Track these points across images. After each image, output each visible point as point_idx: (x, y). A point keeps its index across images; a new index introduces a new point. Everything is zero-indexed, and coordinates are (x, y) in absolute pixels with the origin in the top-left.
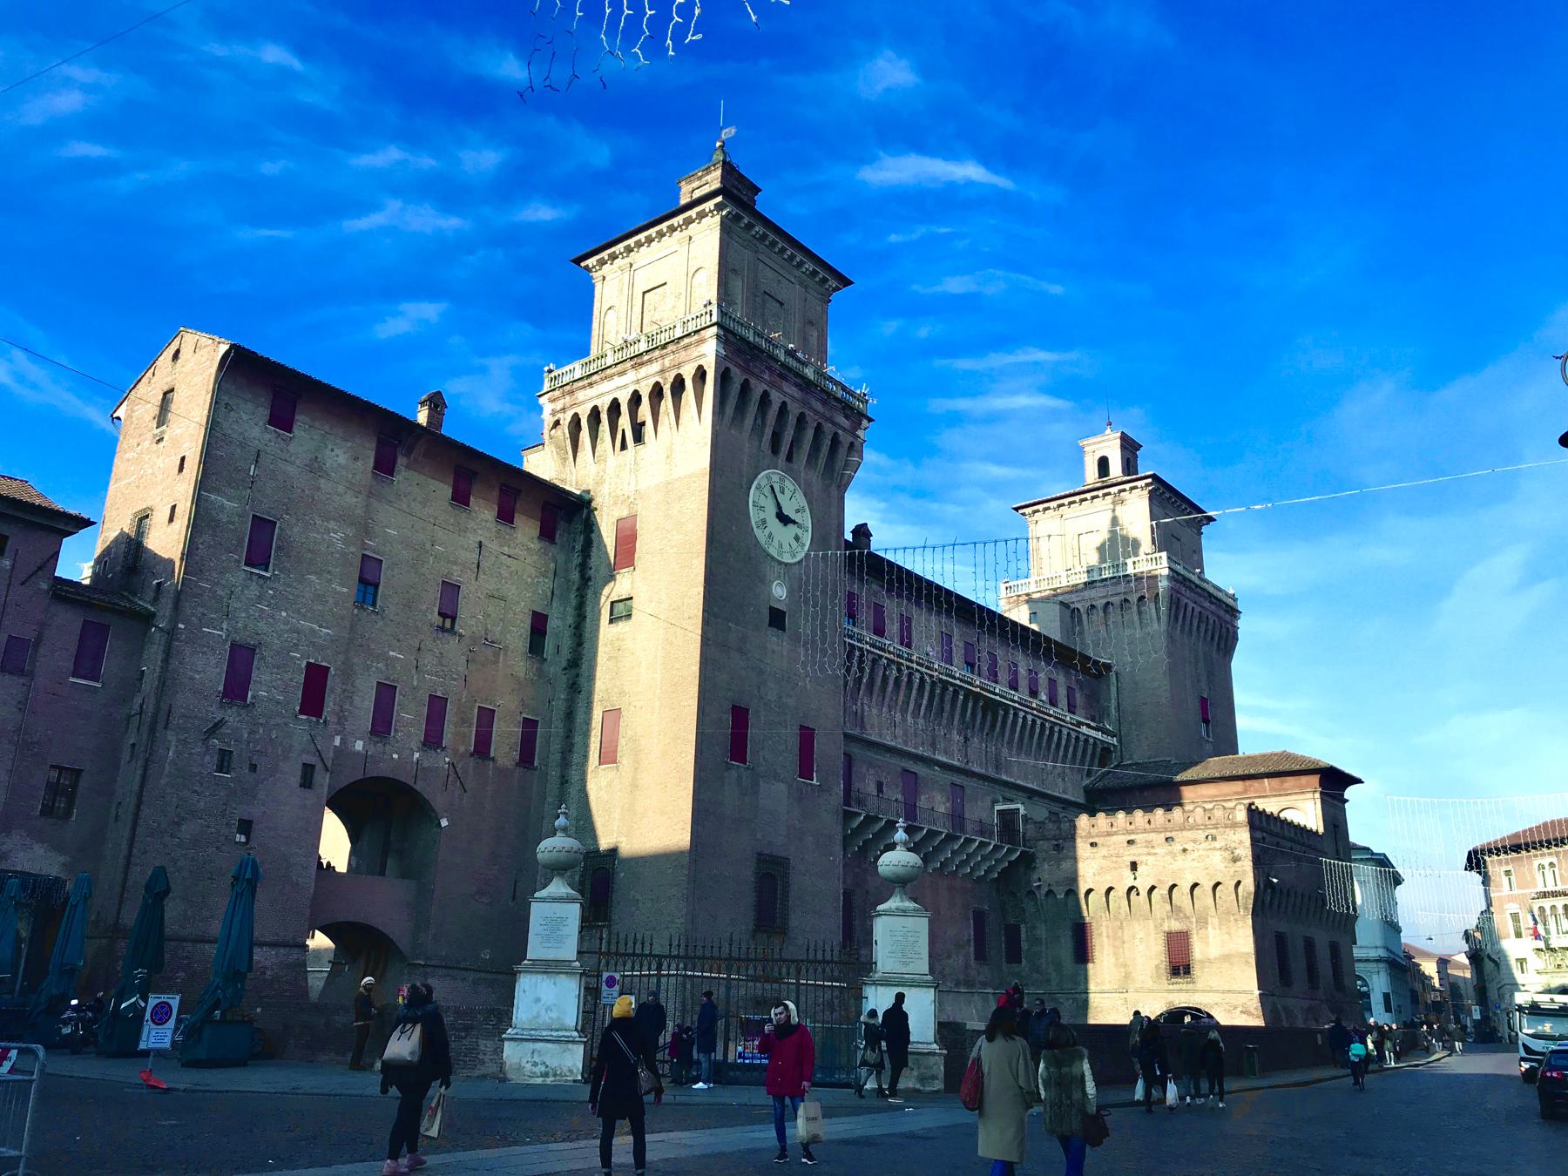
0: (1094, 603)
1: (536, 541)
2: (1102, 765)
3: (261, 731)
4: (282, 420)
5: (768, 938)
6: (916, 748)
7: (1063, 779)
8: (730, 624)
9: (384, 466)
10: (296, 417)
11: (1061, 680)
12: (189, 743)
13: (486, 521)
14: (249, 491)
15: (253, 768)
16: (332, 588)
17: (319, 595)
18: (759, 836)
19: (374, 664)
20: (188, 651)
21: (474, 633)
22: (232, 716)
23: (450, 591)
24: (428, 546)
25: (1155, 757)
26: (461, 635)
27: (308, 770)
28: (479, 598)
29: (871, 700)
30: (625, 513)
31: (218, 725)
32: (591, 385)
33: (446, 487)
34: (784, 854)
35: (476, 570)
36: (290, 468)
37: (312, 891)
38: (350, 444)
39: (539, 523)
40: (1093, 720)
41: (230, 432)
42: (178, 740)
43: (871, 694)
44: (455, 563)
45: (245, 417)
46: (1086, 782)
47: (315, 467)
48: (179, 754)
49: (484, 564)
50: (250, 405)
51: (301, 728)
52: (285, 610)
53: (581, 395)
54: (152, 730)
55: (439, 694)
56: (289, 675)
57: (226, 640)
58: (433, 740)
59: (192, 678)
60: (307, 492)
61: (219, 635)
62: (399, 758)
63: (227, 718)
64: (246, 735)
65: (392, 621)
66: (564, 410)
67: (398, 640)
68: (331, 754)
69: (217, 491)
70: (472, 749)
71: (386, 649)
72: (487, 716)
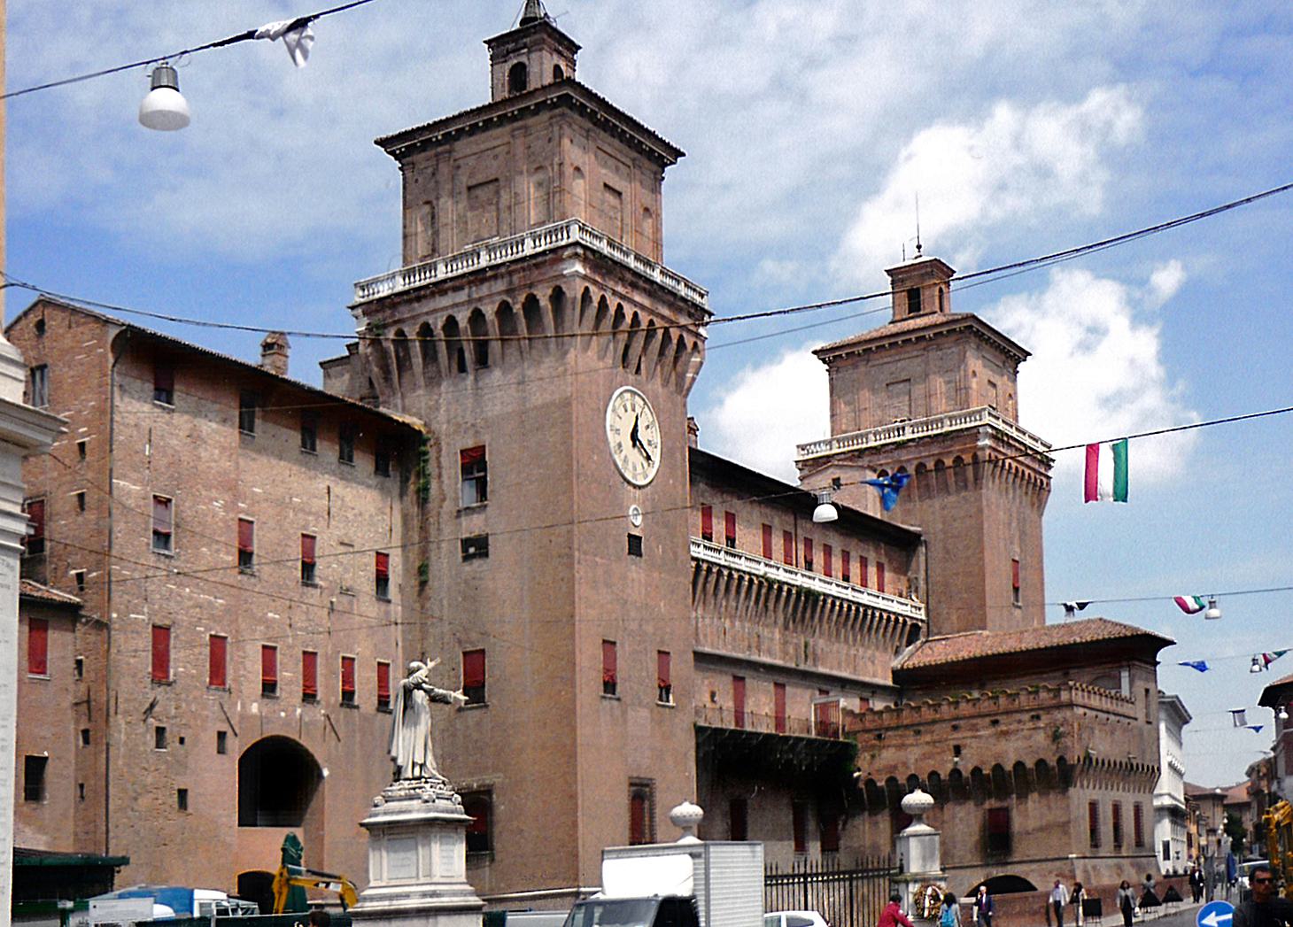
0: (904, 465)
1: (373, 476)
2: (909, 644)
3: (184, 705)
4: (163, 393)
6: (744, 653)
7: (873, 662)
9: (246, 425)
10: (176, 387)
11: (872, 556)
13: (331, 464)
14: (147, 471)
15: (182, 741)
22: (160, 693)
23: (308, 539)
24: (287, 500)
25: (965, 630)
26: (321, 587)
27: (221, 736)
30: (470, 444)
31: (152, 706)
32: (418, 299)
35: (326, 517)
36: (174, 442)
39: (374, 457)
40: (901, 596)
44: (310, 513)
46: (896, 663)
47: (194, 438)
49: (332, 510)
51: (212, 697)
52: (188, 586)
53: (404, 312)
54: (108, 715)
55: (310, 650)
57: (148, 624)
58: (309, 697)
59: (129, 664)
61: (144, 620)
63: (158, 698)
66: (385, 326)
68: (237, 719)
71: (265, 611)
72: (348, 663)
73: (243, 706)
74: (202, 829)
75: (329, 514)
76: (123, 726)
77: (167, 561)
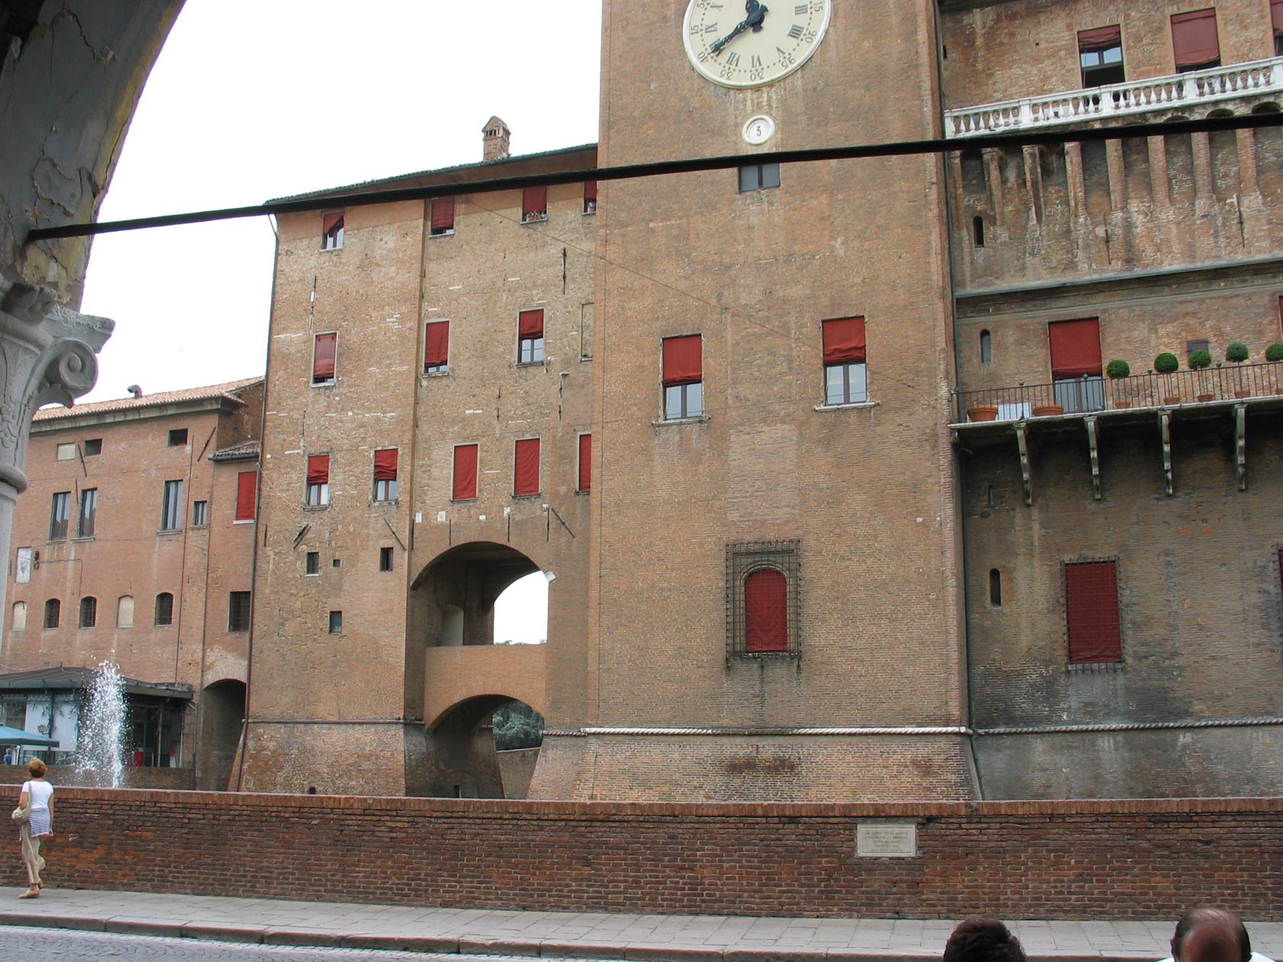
5: (762, 667)
8: (651, 225)
12: (284, 554)
14: (311, 316)
15: (336, 563)
16: (392, 371)
17: (380, 383)
18: (733, 516)
19: (451, 430)
20: (275, 475)
21: (565, 354)
22: (314, 522)
24: (500, 283)
26: (549, 363)
27: (386, 554)
28: (569, 312)
29: (1152, 200)
33: (514, 210)
34: (789, 533)
37: (404, 669)
38: (397, 224)
41: (291, 274)
42: (276, 554)
43: (1149, 188)
44: (535, 286)
45: (302, 254)
48: (276, 564)
50: (306, 242)
52: (352, 409)
55: (528, 437)
56: (358, 471)
57: (304, 455)
60: (361, 292)
62: (486, 519)
63: (311, 525)
64: (327, 535)
65: (465, 378)
67: (474, 396)
69: (285, 329)
70: (577, 486)
73: (425, 517)
74: (358, 650)
75: (564, 277)
76: (272, 557)
77: (328, 391)
